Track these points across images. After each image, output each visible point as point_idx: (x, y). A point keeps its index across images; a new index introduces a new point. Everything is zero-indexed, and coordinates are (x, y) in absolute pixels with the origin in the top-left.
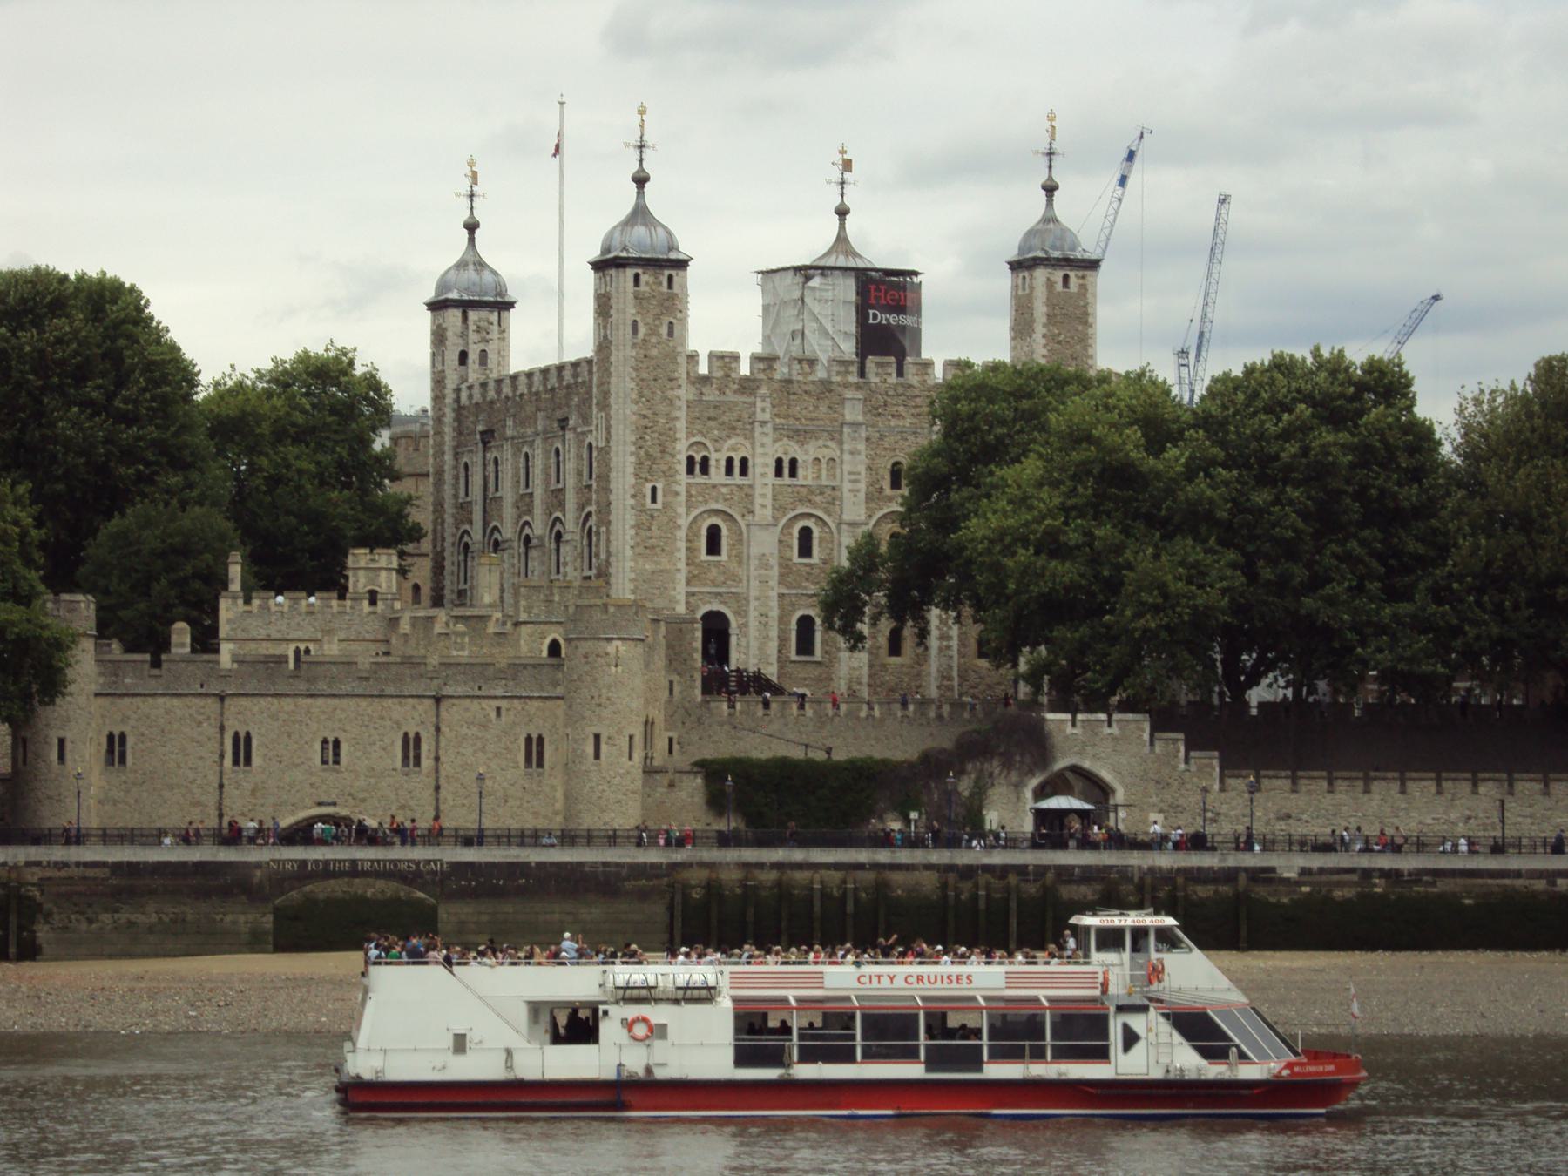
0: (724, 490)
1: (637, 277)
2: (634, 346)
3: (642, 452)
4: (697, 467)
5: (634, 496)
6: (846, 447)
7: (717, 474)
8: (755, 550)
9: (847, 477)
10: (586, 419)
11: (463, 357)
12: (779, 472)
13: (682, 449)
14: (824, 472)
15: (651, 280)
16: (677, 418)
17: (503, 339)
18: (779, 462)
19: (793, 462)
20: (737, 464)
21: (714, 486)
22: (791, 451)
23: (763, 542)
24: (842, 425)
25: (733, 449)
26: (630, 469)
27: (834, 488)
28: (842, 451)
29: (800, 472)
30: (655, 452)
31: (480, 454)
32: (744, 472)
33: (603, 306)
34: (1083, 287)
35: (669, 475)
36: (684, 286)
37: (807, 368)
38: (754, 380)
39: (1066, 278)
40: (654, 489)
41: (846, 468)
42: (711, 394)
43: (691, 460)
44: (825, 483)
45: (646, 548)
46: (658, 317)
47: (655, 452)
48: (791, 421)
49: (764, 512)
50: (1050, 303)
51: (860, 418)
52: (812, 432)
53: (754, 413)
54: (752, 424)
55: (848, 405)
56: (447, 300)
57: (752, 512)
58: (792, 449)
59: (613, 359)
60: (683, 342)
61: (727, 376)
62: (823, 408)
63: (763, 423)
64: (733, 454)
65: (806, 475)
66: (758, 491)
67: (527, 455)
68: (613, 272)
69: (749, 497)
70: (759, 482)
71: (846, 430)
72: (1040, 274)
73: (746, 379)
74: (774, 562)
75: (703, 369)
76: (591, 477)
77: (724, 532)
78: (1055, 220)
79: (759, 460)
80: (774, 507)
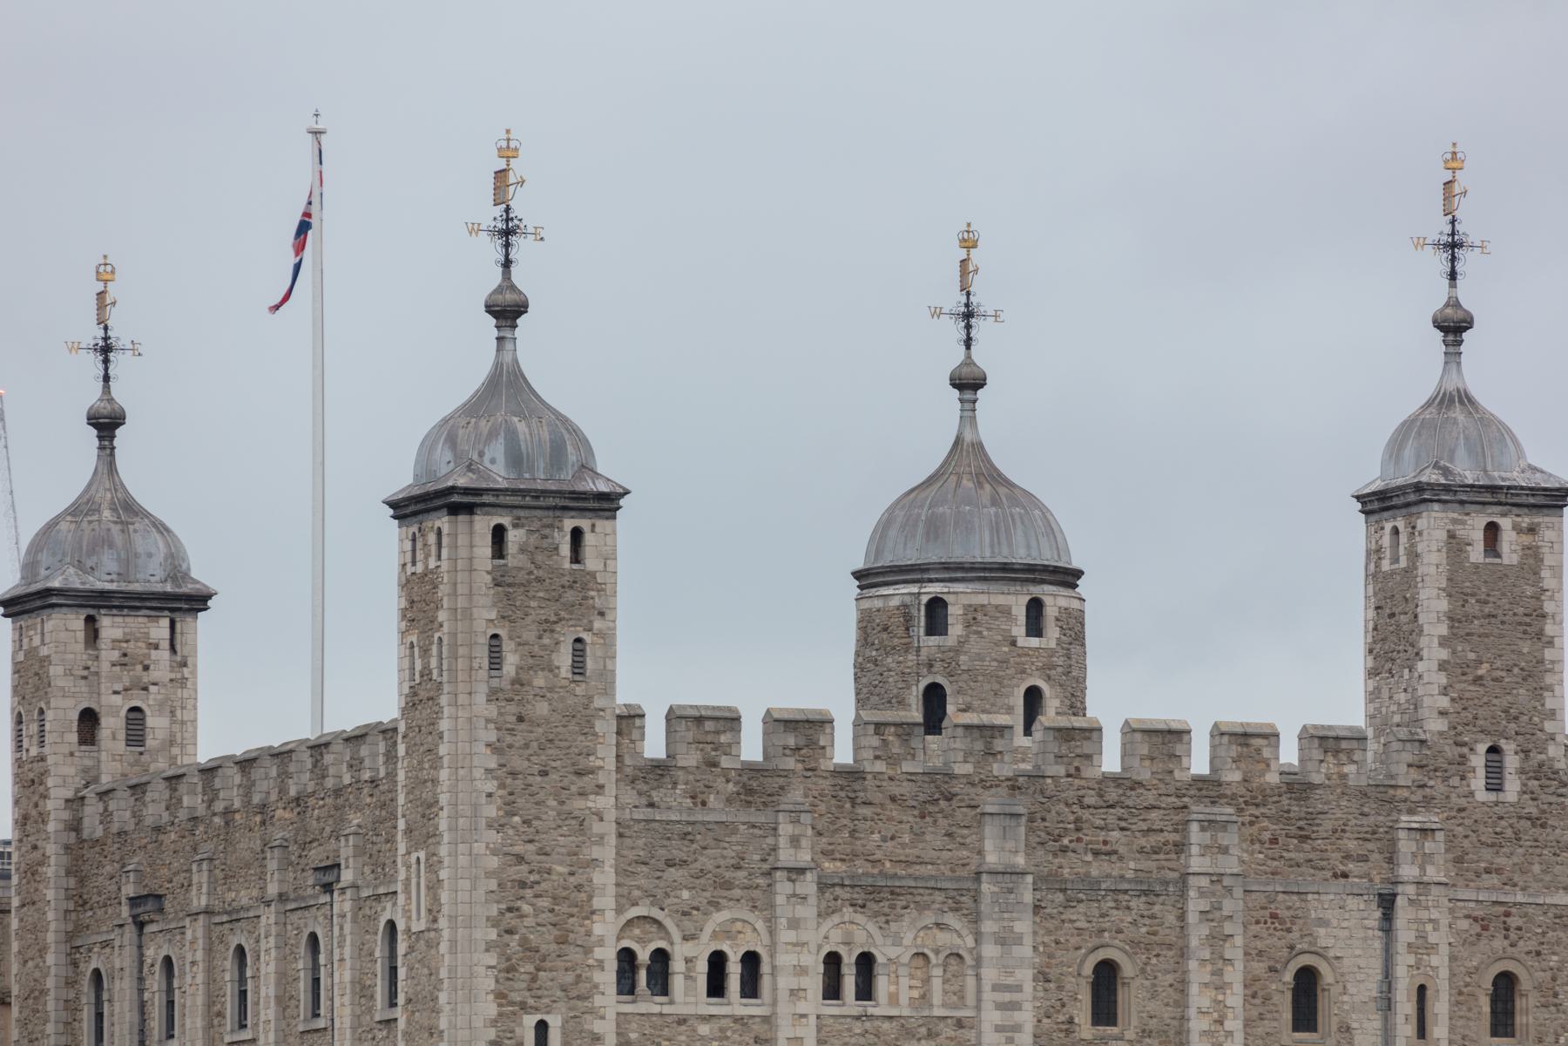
1: (499, 533)
4: (642, 976)
6: (988, 926)
7: (688, 991)
9: (988, 996)
10: (380, 866)
11: (89, 719)
12: (832, 990)
15: (533, 539)
17: (182, 682)
18: (833, 960)
19: (866, 962)
20: (734, 970)
24: (979, 873)
29: (882, 985)
31: (129, 953)
33: (420, 603)
34: (1533, 556)
36: (609, 557)
37: (896, 748)
39: (1492, 530)
41: (989, 975)
44: (938, 1012)
48: (861, 867)
50: (1454, 590)
51: (1020, 860)
53: (774, 849)
54: (768, 874)
56: (48, 592)
59: (444, 725)
61: (715, 765)
62: (934, 838)
64: (725, 947)
67: (240, 951)
68: (443, 522)
70: (784, 1009)
72: (1433, 523)
75: (654, 745)
76: (393, 1004)
78: (1463, 399)
79: (785, 959)
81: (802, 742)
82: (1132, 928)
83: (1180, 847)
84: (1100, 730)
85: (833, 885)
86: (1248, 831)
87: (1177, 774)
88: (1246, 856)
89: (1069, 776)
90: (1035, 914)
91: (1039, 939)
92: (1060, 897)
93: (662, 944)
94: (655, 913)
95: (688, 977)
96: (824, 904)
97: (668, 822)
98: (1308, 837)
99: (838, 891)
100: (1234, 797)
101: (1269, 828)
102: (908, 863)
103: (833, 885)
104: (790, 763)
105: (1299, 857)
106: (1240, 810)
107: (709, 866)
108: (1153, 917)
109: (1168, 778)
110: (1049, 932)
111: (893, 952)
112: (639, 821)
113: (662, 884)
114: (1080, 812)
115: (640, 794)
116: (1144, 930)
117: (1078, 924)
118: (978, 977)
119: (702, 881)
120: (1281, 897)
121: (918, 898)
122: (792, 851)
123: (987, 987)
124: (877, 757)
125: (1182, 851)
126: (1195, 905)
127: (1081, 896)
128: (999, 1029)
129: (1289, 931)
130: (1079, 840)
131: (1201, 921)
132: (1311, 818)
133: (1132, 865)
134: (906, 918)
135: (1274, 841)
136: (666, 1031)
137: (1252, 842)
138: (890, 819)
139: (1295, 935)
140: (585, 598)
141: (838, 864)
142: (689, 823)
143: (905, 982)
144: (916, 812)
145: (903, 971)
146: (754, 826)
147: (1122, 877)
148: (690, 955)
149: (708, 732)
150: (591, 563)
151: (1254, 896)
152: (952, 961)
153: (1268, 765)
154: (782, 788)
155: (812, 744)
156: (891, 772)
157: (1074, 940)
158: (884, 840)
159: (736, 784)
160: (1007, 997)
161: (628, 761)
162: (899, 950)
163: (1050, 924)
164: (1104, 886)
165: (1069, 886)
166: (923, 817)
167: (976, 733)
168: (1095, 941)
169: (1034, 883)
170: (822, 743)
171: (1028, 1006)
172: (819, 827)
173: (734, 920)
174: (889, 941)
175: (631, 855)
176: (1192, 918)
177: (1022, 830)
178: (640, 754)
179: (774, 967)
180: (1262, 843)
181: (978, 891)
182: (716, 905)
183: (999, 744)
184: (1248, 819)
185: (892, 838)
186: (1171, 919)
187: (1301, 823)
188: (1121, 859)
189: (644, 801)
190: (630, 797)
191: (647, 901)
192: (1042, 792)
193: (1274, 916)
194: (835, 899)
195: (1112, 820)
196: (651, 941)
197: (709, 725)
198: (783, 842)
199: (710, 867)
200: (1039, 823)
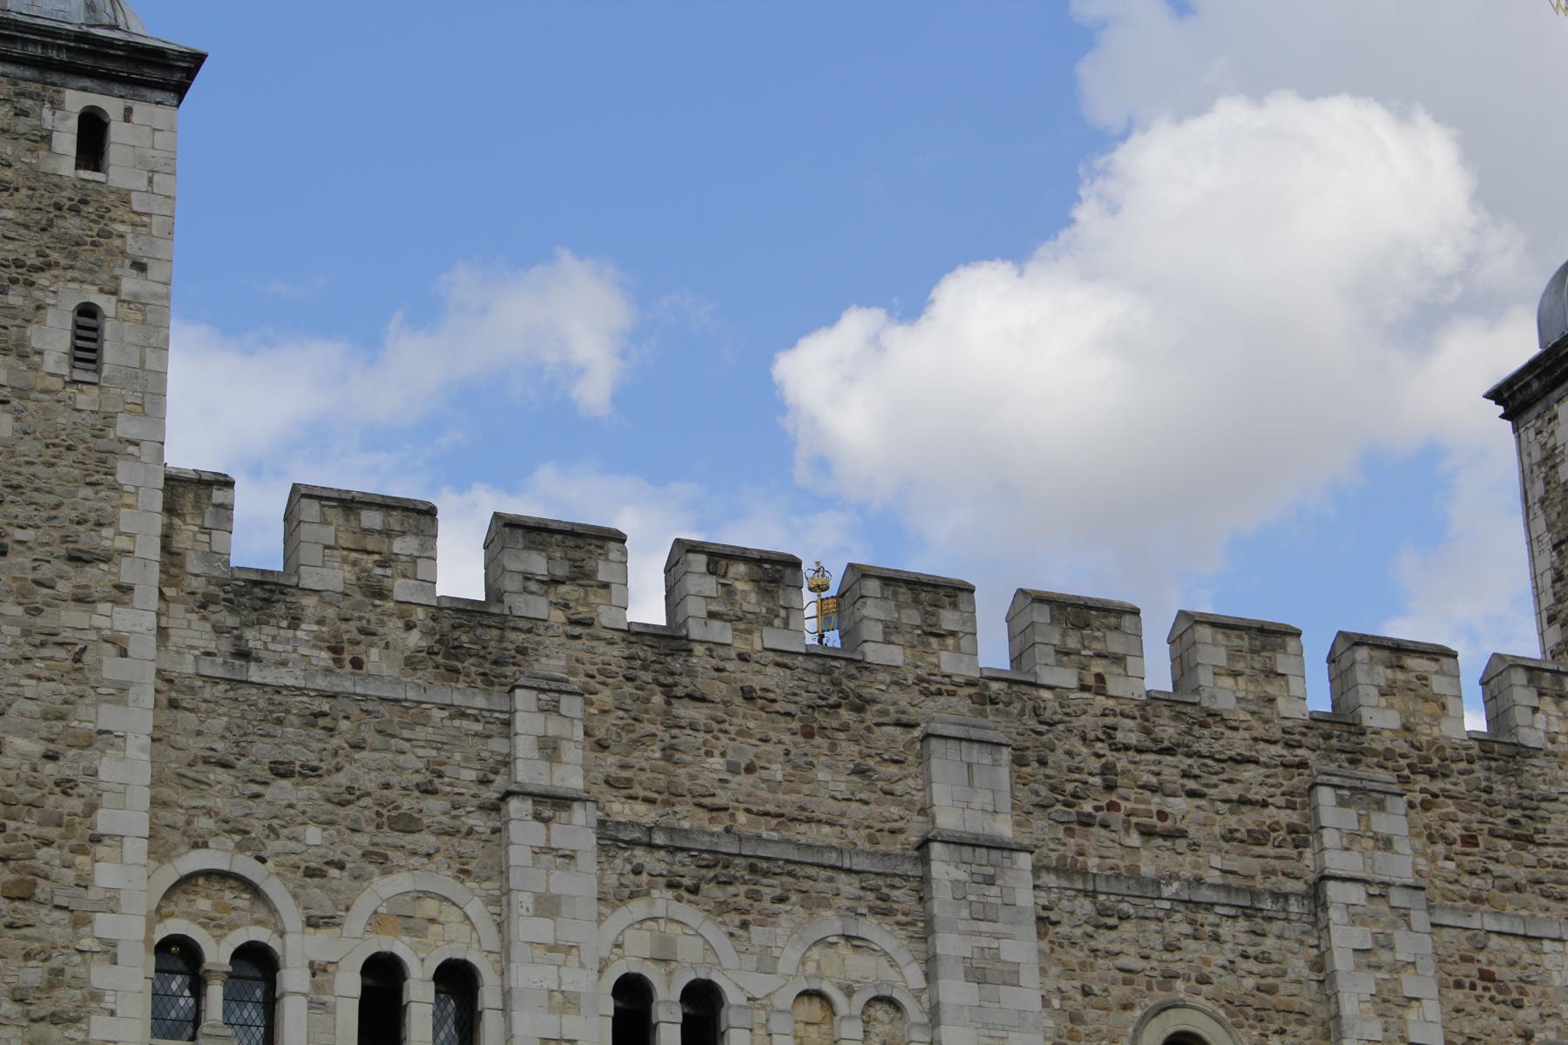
4: (215, 993)
6: (949, 944)
13: (127, 897)
24: (924, 845)
25: (406, 922)
37: (750, 599)
38: (504, 623)
51: (1004, 828)
52: (790, 868)
53: (507, 762)
54: (495, 808)
55: (945, 764)
60: (149, 396)
61: (380, 593)
63: (553, 802)
64: (400, 947)
71: (944, 868)
73: (464, 611)
75: (255, 538)
79: (530, 976)
81: (561, 571)
82: (1228, 978)
83: (1301, 836)
85: (633, 843)
87: (1283, 706)
88: (1422, 864)
89: (1084, 688)
90: (1041, 936)
91: (1051, 984)
92: (1085, 907)
94: (245, 865)
95: (315, 1005)
96: (612, 879)
98: (1529, 840)
99: (640, 855)
100: (1389, 754)
102: (782, 818)
103: (633, 843)
104: (537, 606)
105: (1521, 875)
106: (1404, 780)
107: (369, 782)
108: (1263, 958)
109: (1267, 712)
110: (1069, 972)
111: (759, 985)
112: (215, 680)
113: (259, 808)
114: (1111, 756)
115: (218, 630)
116: (1249, 983)
117: (1123, 961)
119: (351, 811)
120: (1494, 941)
121: (806, 885)
122: (543, 765)
124: (712, 615)
125: (1306, 844)
126: (1345, 938)
127: (1124, 906)
129: (1518, 1005)
130: (1113, 806)
131: (1358, 967)
132: (1530, 805)
133: (1216, 860)
134: (783, 918)
135: (1470, 840)
137: (1431, 839)
138: (744, 733)
139: (1528, 1015)
140: (109, 235)
141: (641, 808)
142: (323, 694)
144: (796, 725)
145: (777, 1023)
146: (463, 715)
147: (1199, 881)
148: (321, 958)
149: (369, 532)
150: (120, 170)
151: (1446, 935)
152: (880, 1012)
153: (1444, 707)
154: (522, 651)
155: (581, 575)
156: (740, 646)
157: (1119, 992)
158: (733, 768)
161: (193, 565)
163: (1076, 956)
164: (1167, 891)
165: (1101, 886)
166: (808, 734)
167: (905, 594)
168: (1160, 996)
169: (1036, 870)
170: (602, 577)
172: (600, 733)
173: (422, 895)
175: (196, 746)
176: (1342, 961)
177: (1004, 774)
178: (217, 556)
179: (506, 995)
180: (1450, 843)
181: (925, 880)
182: (378, 858)
183: (948, 619)
185: (750, 769)
186: (1298, 966)
187: (1511, 814)
188: (1194, 847)
189: (225, 645)
190: (193, 633)
191: (230, 842)
192: (1036, 712)
193: (1486, 976)
194: (637, 871)
195: (1171, 775)
196: (233, 926)
197: (372, 519)
198: (524, 747)
199: (371, 787)
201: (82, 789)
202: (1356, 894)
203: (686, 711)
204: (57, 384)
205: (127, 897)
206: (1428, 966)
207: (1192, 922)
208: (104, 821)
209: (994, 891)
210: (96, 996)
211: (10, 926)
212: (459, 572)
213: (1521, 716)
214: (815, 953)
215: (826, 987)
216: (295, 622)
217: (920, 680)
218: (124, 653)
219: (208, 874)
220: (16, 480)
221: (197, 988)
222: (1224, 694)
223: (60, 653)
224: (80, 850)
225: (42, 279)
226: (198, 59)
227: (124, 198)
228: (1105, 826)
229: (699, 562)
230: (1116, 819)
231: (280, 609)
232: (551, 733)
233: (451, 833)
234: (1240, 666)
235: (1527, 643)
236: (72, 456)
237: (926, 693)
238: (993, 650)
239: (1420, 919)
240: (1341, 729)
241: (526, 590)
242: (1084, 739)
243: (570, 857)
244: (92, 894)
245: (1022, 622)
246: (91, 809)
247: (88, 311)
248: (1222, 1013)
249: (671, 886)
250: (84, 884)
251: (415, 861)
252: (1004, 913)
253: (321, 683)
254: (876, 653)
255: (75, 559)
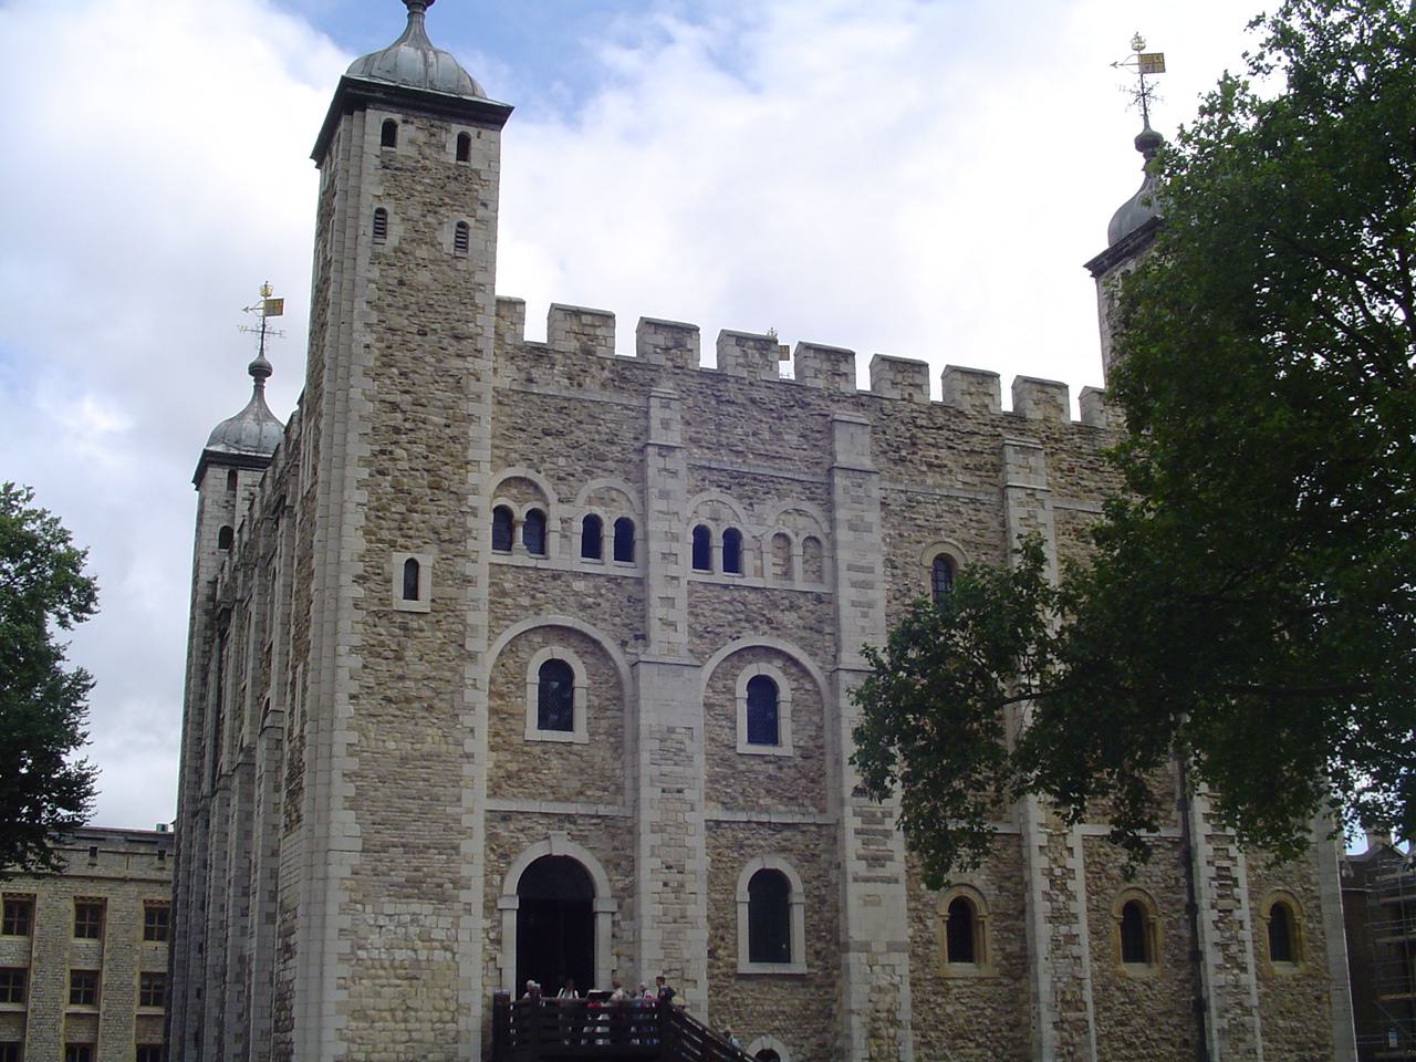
0: (579, 585)
2: (376, 258)
3: (386, 482)
4: (519, 532)
5: (360, 579)
6: (841, 514)
7: (564, 552)
8: (648, 719)
9: (844, 575)
12: (701, 559)
13: (484, 487)
14: (798, 563)
16: (469, 418)
18: (701, 535)
19: (732, 539)
21: (556, 576)
22: (725, 513)
23: (678, 700)
24: (830, 471)
25: (601, 500)
26: (355, 519)
27: (819, 599)
28: (832, 522)
29: (748, 559)
30: (419, 485)
32: (624, 551)
35: (451, 542)
36: (494, 160)
37: (756, 357)
38: (646, 367)
40: (412, 566)
41: (844, 556)
42: (552, 382)
43: (503, 516)
44: (800, 585)
45: (392, 701)
46: (431, 208)
47: (419, 485)
49: (671, 631)
51: (868, 464)
52: (772, 479)
53: (647, 430)
54: (641, 451)
57: (642, 637)
58: (724, 511)
61: (591, 353)
62: (792, 438)
64: (598, 511)
65: (760, 569)
66: (657, 589)
69: (639, 603)
70: (657, 572)
71: (840, 480)
74: (697, 749)
77: (581, 678)
79: (656, 526)
80: (692, 631)
81: (670, 344)
82: (965, 530)
83: (998, 468)
84: (927, 365)
86: (1049, 461)
89: (904, 400)
91: (886, 531)
93: (538, 505)
96: (693, 482)
97: (545, 396)
101: (1067, 461)
104: (661, 360)
106: (1043, 443)
107: (583, 438)
108: (978, 521)
112: (518, 392)
114: (914, 430)
116: (973, 532)
117: (918, 522)
118: (834, 559)
120: (1080, 514)
121: (779, 486)
123: (842, 566)
128: (854, 604)
130: (914, 453)
133: (960, 477)
135: (1071, 470)
136: (541, 585)
141: (706, 451)
142: (565, 399)
143: (768, 559)
146: (626, 408)
148: (566, 516)
149: (584, 325)
150: (476, 161)
152: (810, 544)
155: (679, 345)
159: (611, 372)
160: (861, 576)
162: (762, 529)
163: (895, 520)
166: (780, 419)
167: (823, 356)
171: (877, 585)
172: (687, 417)
174: (754, 520)
177: (867, 439)
180: (1062, 471)
183: (843, 368)
184: (1049, 451)
186: (995, 524)
187: (1091, 458)
189: (523, 375)
194: (703, 480)
197: (586, 319)
198: (655, 423)
200: (881, 436)
201: (462, 440)
202: (1021, 494)
203: (723, 407)
204: (445, 257)
205: (484, 487)
206: (1051, 523)
207: (948, 505)
208: (472, 454)
209: (861, 490)
210: (470, 532)
211: (432, 500)
212: (625, 344)
213: (1096, 414)
214: (782, 517)
215: (787, 531)
216: (553, 366)
217: (830, 395)
218: (478, 380)
219: (515, 478)
220: (431, 302)
221: (511, 529)
222: (966, 404)
223: (451, 380)
224: (460, 467)
225: (442, 210)
226: (510, 109)
227: (477, 172)
228: (911, 461)
229: (733, 341)
230: (916, 458)
231: (546, 360)
232: (667, 416)
233: (622, 461)
234: (973, 390)
235: (1099, 383)
236: (453, 291)
237: (832, 400)
238: (863, 382)
239: (1049, 504)
240: (1017, 419)
241: (656, 352)
242: (902, 422)
243: (675, 473)
244: (467, 486)
245: (877, 369)
246: (465, 449)
247: (462, 225)
248: (960, 546)
249: (719, 486)
250: (462, 482)
251: (605, 474)
252: (865, 500)
253: (565, 393)
254: (809, 383)
255: (457, 338)
